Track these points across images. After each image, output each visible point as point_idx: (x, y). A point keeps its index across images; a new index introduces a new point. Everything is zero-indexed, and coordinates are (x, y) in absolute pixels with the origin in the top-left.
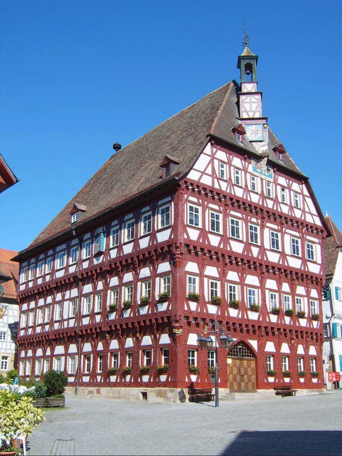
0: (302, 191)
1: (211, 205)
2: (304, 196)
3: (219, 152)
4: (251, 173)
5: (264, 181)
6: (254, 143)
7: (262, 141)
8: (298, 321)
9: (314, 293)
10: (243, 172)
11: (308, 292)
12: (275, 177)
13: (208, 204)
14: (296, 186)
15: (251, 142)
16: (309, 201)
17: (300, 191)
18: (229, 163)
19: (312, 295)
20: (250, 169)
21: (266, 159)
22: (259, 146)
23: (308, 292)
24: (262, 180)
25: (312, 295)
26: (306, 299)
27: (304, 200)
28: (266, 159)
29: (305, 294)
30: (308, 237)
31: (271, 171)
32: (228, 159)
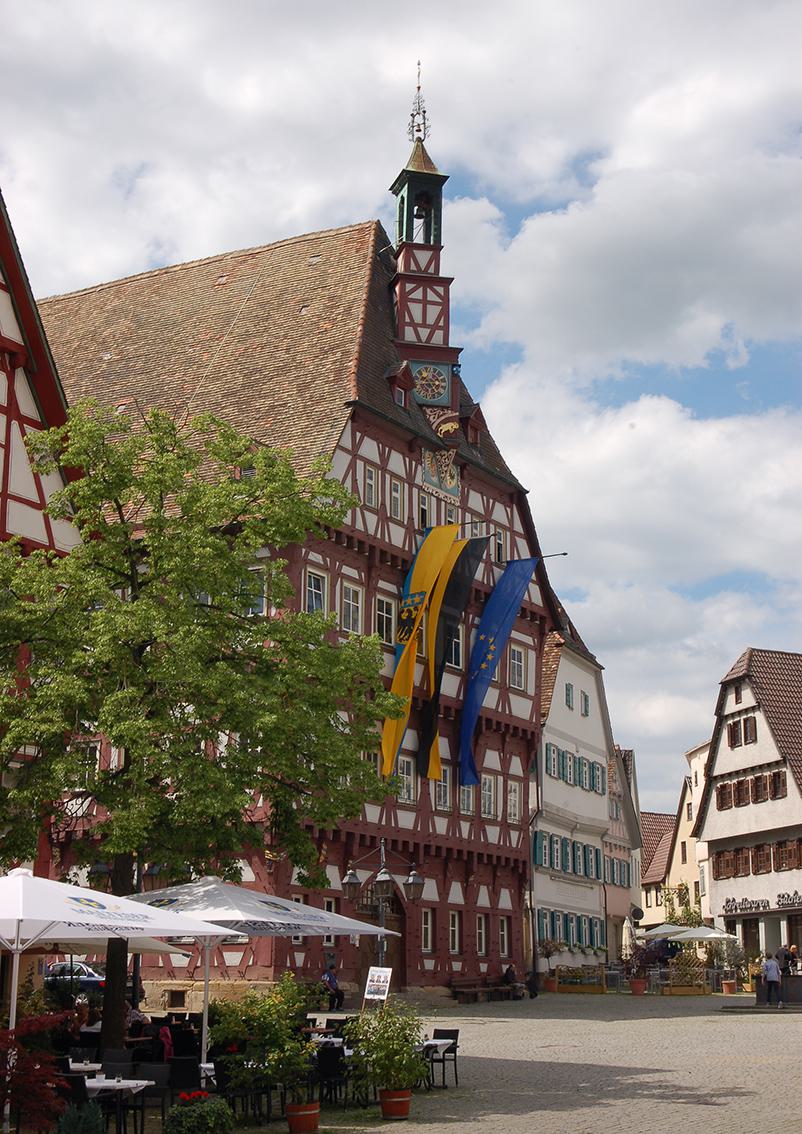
0: (511, 521)
1: (346, 570)
2: (514, 533)
3: (366, 440)
4: (420, 488)
5: (443, 503)
6: (428, 411)
7: (447, 408)
8: (484, 830)
9: (516, 766)
10: (406, 485)
11: (505, 763)
12: (463, 492)
13: (340, 567)
14: (500, 513)
15: (421, 406)
16: (522, 544)
17: (507, 524)
18: (383, 467)
19: (511, 772)
20: (418, 480)
21: (452, 452)
22: (439, 421)
23: (505, 763)
24: (439, 500)
25: (511, 772)
26: (501, 779)
27: (514, 544)
28: (452, 452)
29: (498, 767)
30: (515, 634)
31: (455, 480)
32: (381, 455)
